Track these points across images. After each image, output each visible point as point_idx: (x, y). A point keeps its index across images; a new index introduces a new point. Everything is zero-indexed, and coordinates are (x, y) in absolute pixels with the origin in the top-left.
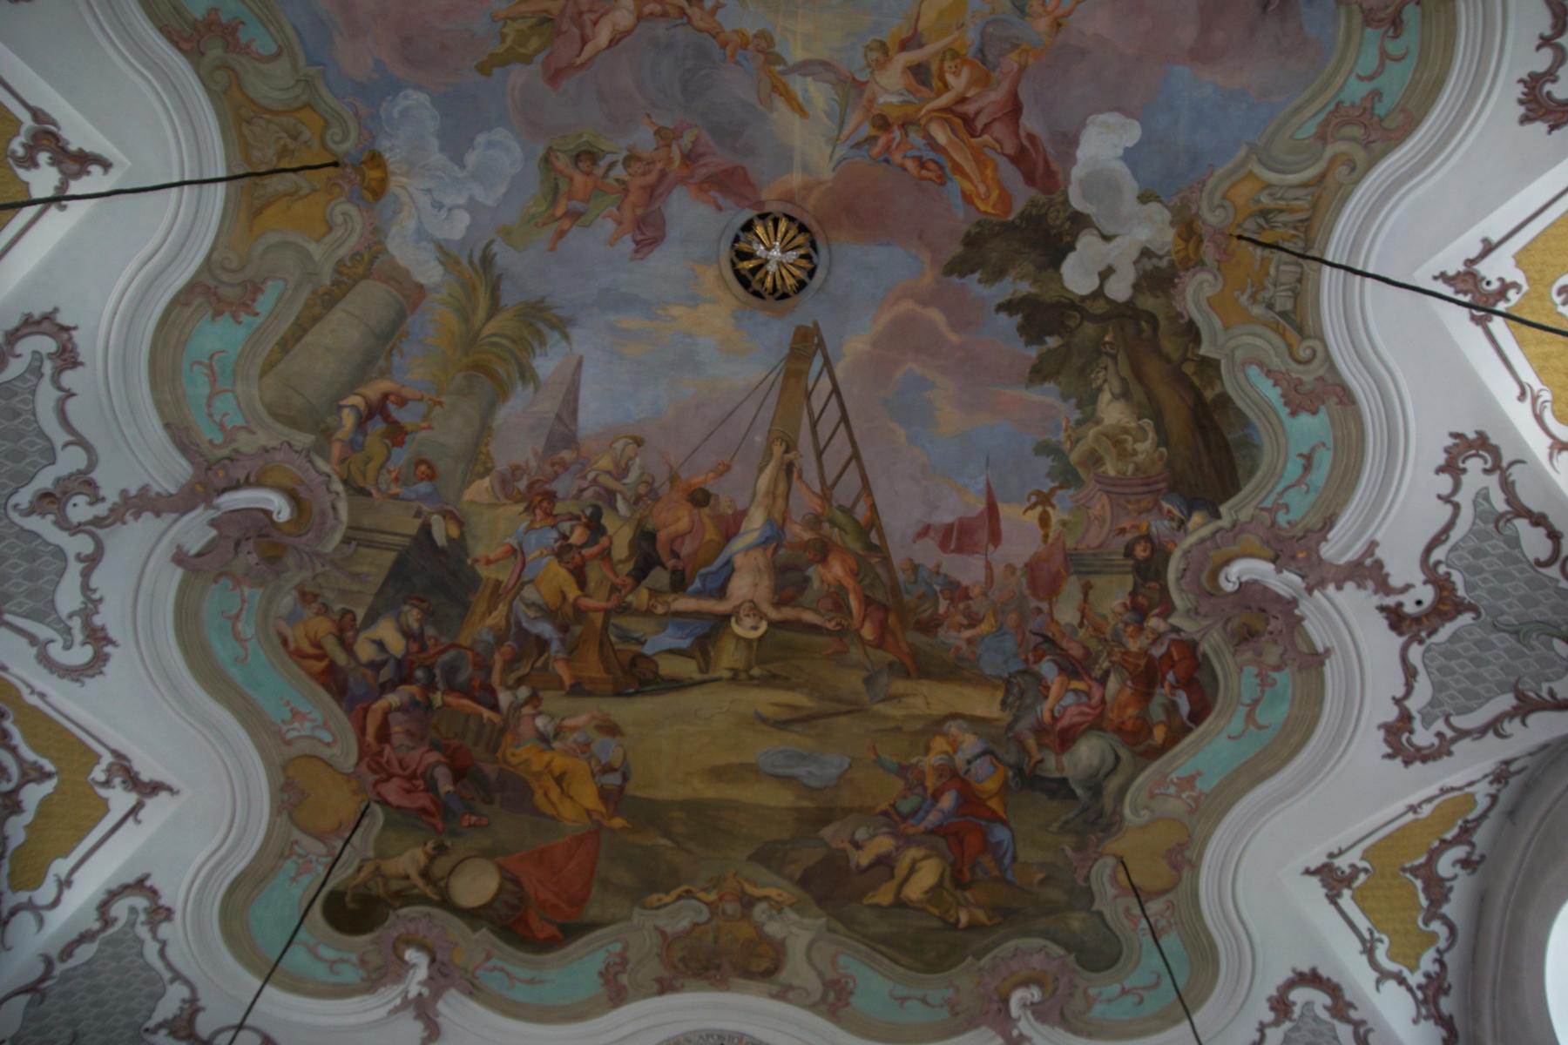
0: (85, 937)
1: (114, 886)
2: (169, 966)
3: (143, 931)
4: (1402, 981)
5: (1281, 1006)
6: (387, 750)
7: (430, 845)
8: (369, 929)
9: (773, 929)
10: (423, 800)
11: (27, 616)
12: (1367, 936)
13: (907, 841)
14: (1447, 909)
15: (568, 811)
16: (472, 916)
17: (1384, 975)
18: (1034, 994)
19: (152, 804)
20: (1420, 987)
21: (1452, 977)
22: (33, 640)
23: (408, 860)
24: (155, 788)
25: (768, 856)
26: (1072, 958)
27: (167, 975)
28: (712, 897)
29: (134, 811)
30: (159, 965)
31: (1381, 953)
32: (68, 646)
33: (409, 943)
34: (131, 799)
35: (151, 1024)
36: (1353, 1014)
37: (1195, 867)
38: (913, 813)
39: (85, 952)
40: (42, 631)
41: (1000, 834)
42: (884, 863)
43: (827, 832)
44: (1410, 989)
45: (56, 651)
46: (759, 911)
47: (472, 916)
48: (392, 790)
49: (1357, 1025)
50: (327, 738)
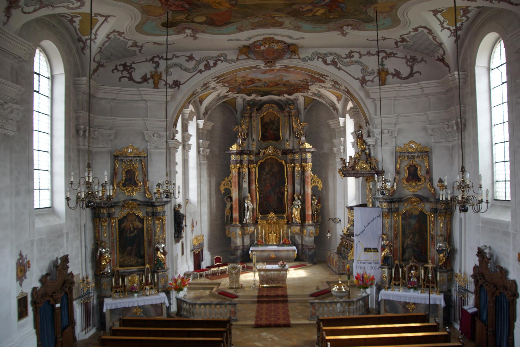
0: (105, 42)
1: (108, 33)
2: (127, 39)
3: (119, 37)
4: (449, 29)
5: (416, 30)
6: (169, 3)
7: (186, 15)
8: (175, 26)
9: (281, 20)
10: (181, 9)
11: (60, 3)
12: (442, 21)
13: (316, 7)
14: (468, 15)
15: (222, 8)
16: (201, 23)
17: (444, 28)
18: (350, 28)
19: (109, 19)
20: (453, 30)
21: (463, 27)
22: (64, 7)
23: (182, 17)
24: (109, 16)
25: (278, 10)
26: (361, 21)
27: (127, 41)
28: (264, 17)
29: (106, 20)
30: (125, 40)
31: (445, 25)
32: (73, 4)
33: (186, 28)
34: (104, 18)
35: (128, 46)
36: (433, 34)
37: (397, 9)
38: (318, 3)
39: (106, 44)
40: (65, 4)
41: (342, 5)
42: (311, 10)
43: (294, 7)
44: (451, 31)
45: (71, 6)
46: (276, 18)
47: (201, 23)
48: (173, 8)
49: (433, 37)
50: (151, 2)
